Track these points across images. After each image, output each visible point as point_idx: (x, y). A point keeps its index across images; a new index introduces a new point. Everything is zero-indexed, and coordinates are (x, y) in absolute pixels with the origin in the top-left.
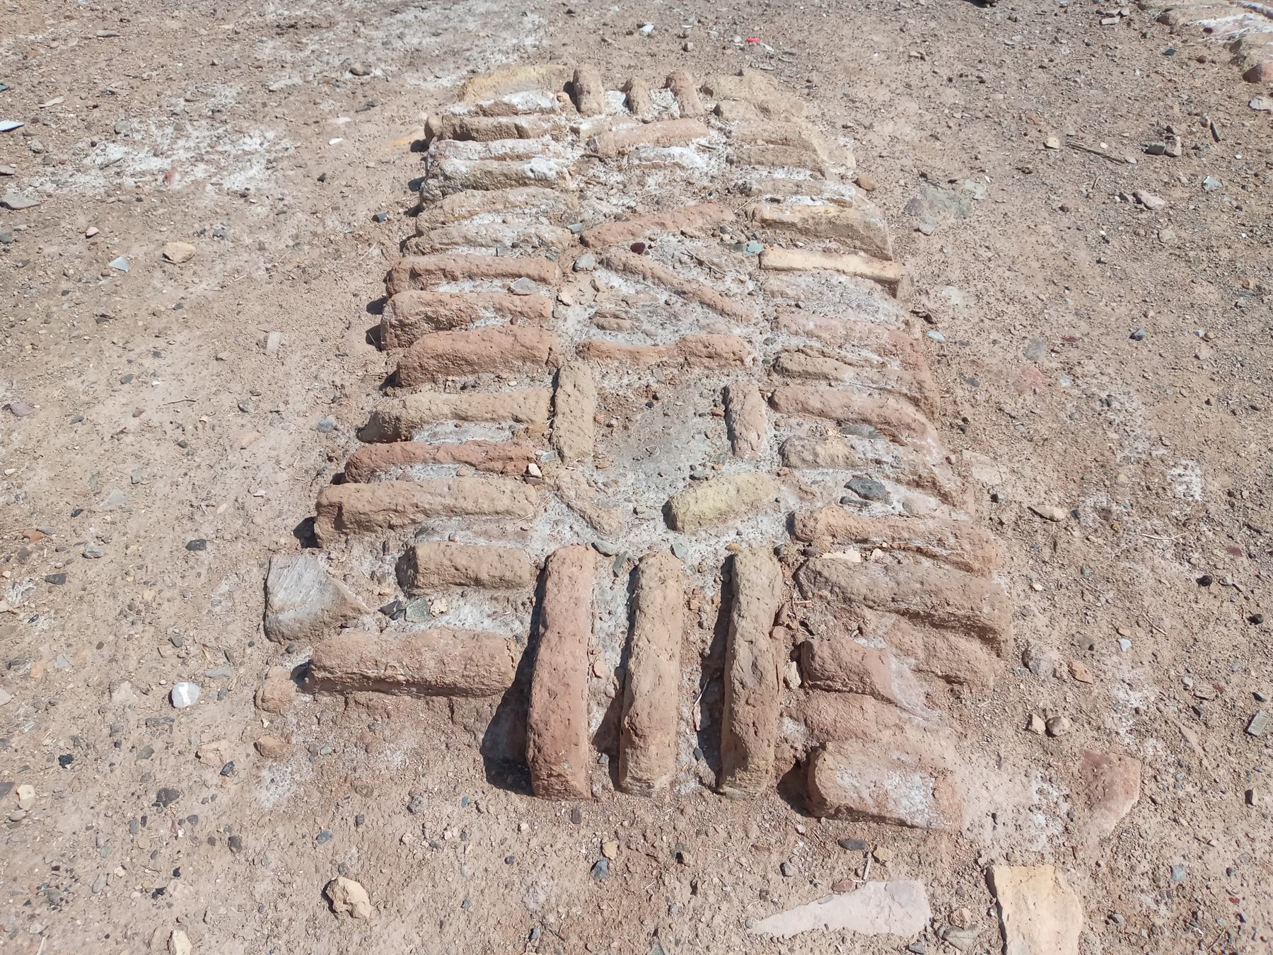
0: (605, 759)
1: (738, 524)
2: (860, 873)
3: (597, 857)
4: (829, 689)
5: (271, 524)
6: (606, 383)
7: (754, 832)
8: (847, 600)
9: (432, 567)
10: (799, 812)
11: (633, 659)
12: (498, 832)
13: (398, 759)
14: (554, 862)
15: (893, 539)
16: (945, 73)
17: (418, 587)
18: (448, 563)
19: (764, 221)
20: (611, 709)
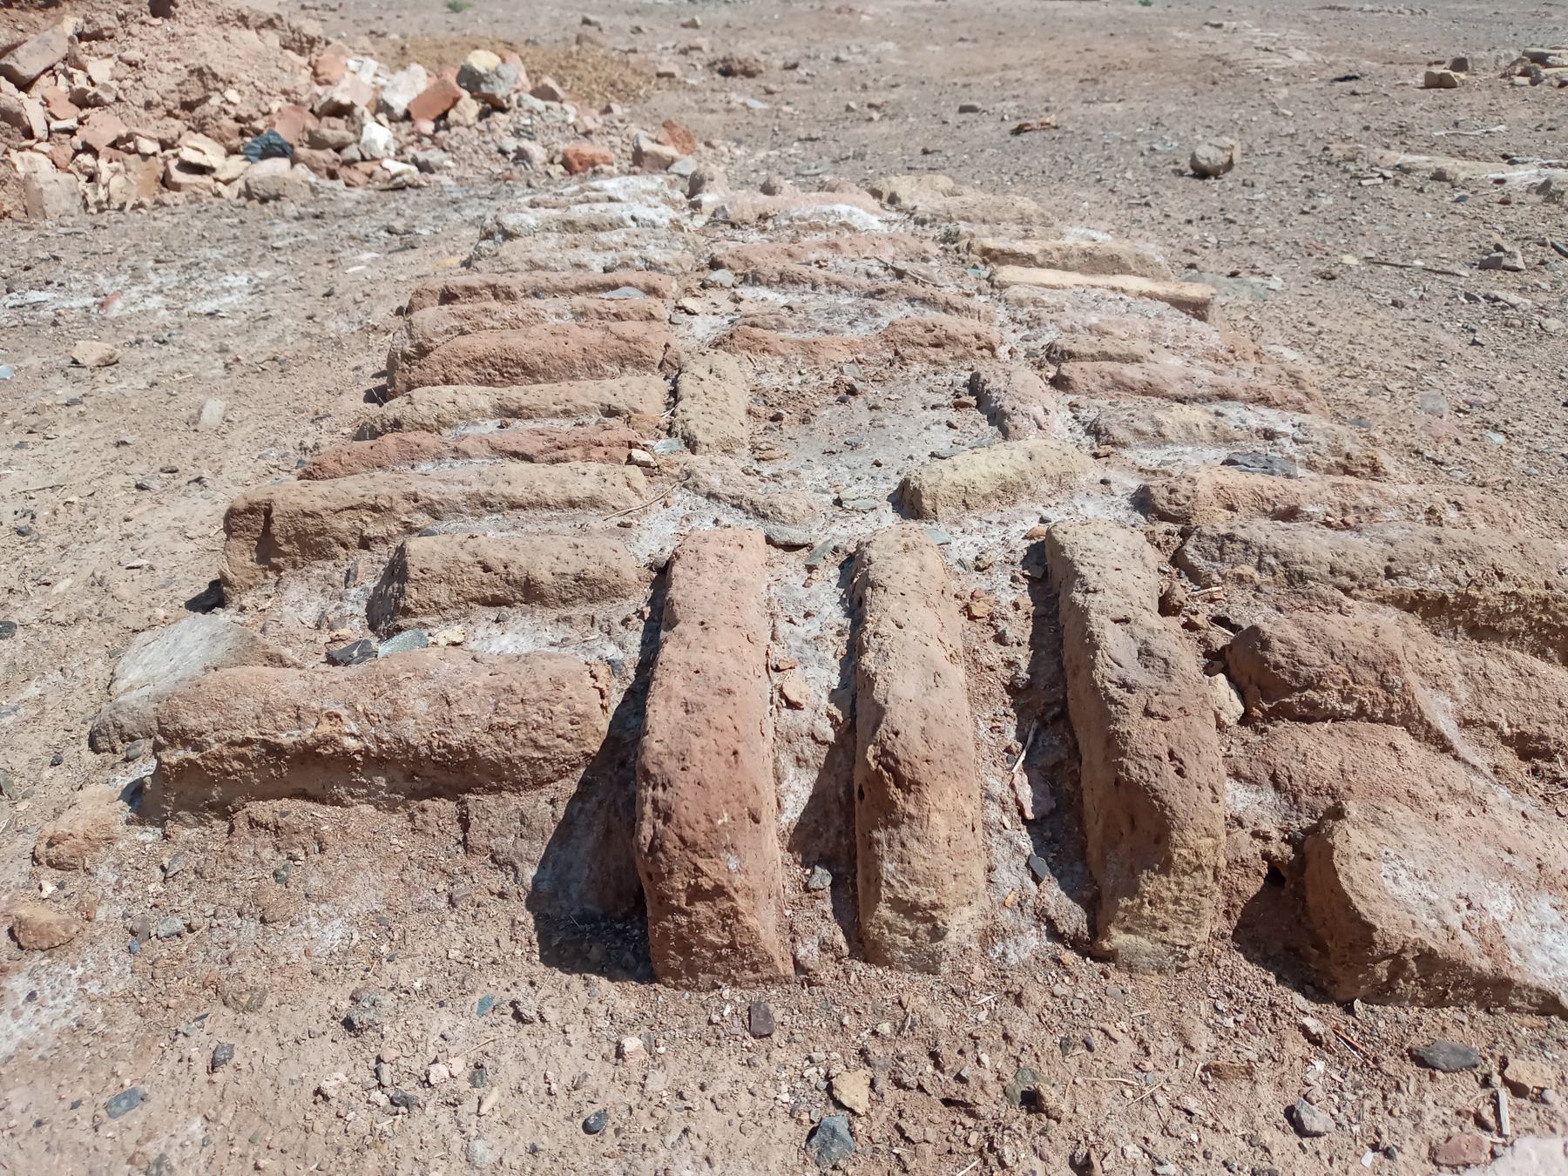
0: (822, 878)
1: (1039, 508)
2: (1492, 1122)
3: (819, 1110)
4: (1312, 715)
5: (147, 598)
6: (764, 380)
7: (1203, 1039)
8: (1296, 578)
9: (437, 567)
10: (1299, 989)
11: (871, 654)
12: (566, 1062)
13: (333, 935)
14: (709, 1123)
15: (1345, 510)
16: (1183, 218)
17: (407, 612)
18: (469, 559)
19: (986, 252)
20: (825, 771)
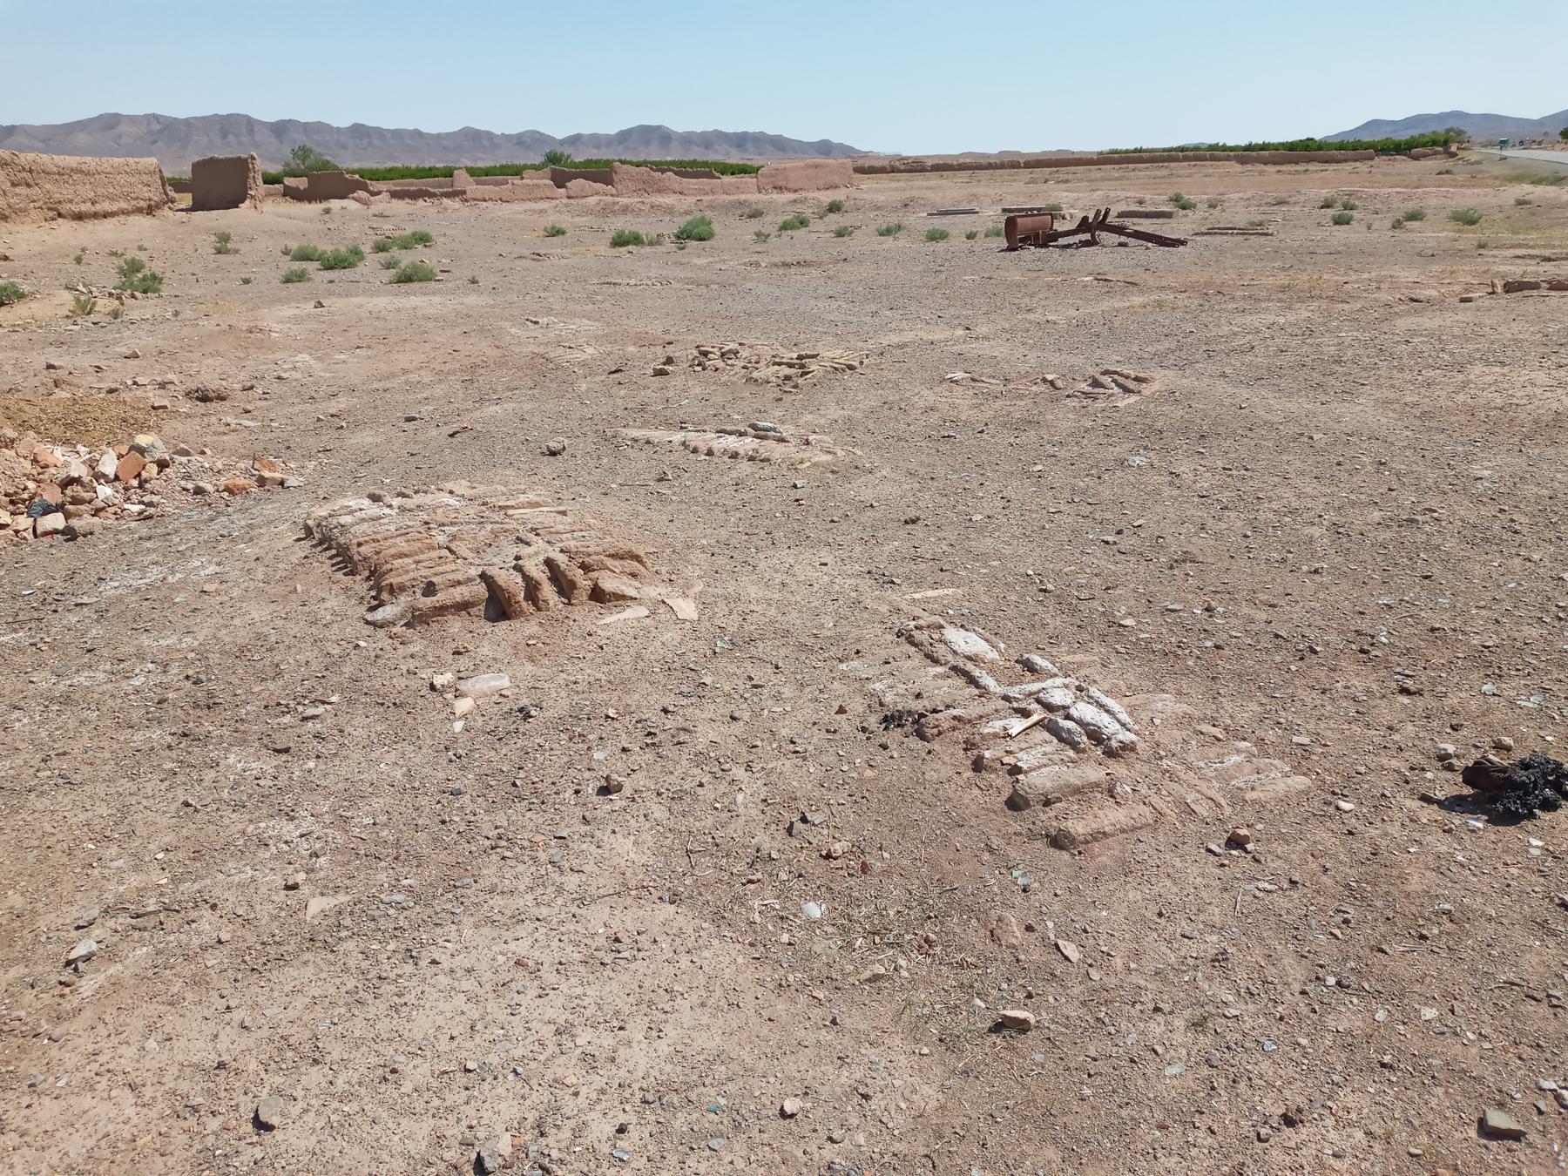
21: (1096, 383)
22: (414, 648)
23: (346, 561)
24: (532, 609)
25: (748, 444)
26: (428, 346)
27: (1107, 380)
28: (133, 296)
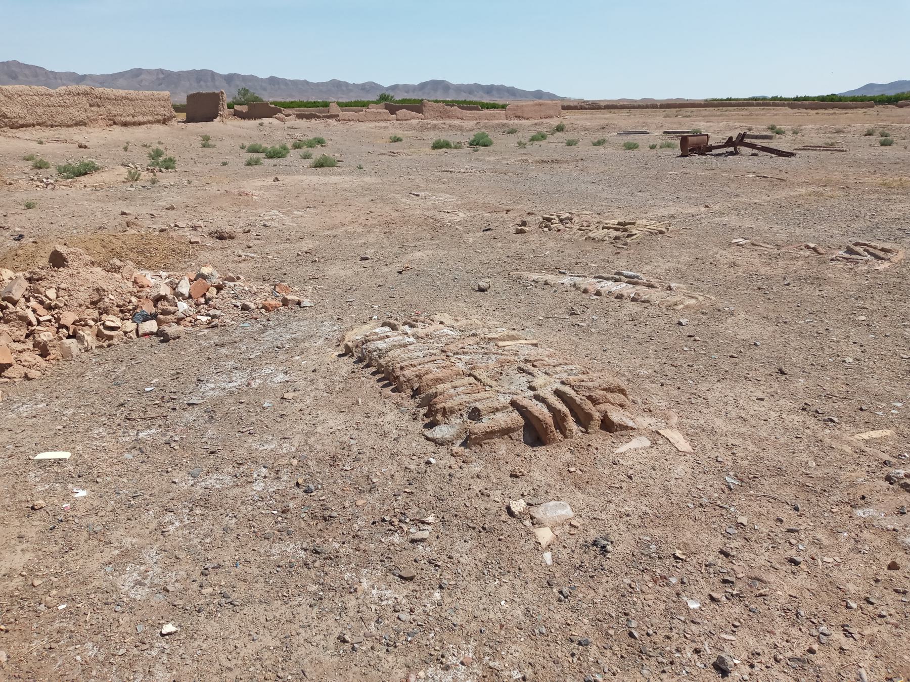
4: (599, 403)
8: (589, 389)
21: (850, 251)
22: (476, 467)
23: (389, 378)
24: (559, 436)
25: (623, 287)
26: (353, 209)
27: (857, 248)
28: (161, 171)
